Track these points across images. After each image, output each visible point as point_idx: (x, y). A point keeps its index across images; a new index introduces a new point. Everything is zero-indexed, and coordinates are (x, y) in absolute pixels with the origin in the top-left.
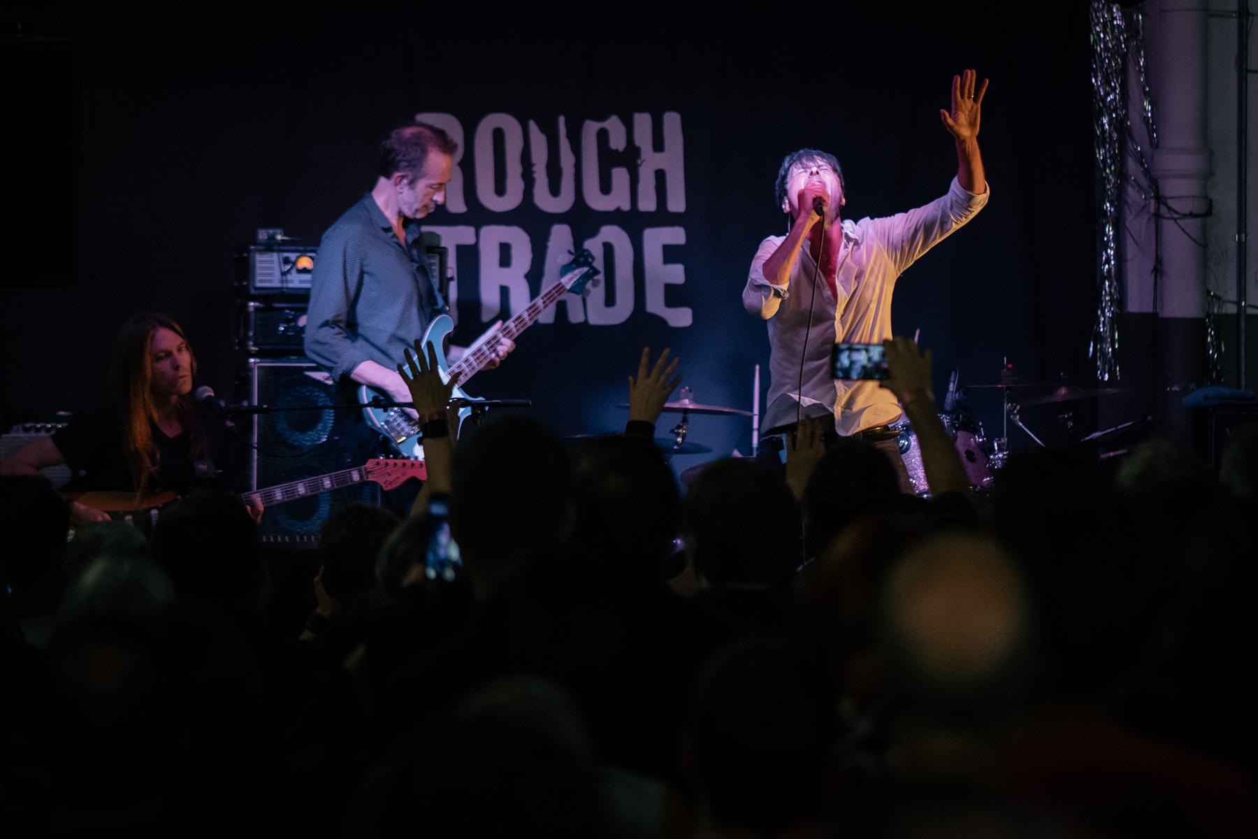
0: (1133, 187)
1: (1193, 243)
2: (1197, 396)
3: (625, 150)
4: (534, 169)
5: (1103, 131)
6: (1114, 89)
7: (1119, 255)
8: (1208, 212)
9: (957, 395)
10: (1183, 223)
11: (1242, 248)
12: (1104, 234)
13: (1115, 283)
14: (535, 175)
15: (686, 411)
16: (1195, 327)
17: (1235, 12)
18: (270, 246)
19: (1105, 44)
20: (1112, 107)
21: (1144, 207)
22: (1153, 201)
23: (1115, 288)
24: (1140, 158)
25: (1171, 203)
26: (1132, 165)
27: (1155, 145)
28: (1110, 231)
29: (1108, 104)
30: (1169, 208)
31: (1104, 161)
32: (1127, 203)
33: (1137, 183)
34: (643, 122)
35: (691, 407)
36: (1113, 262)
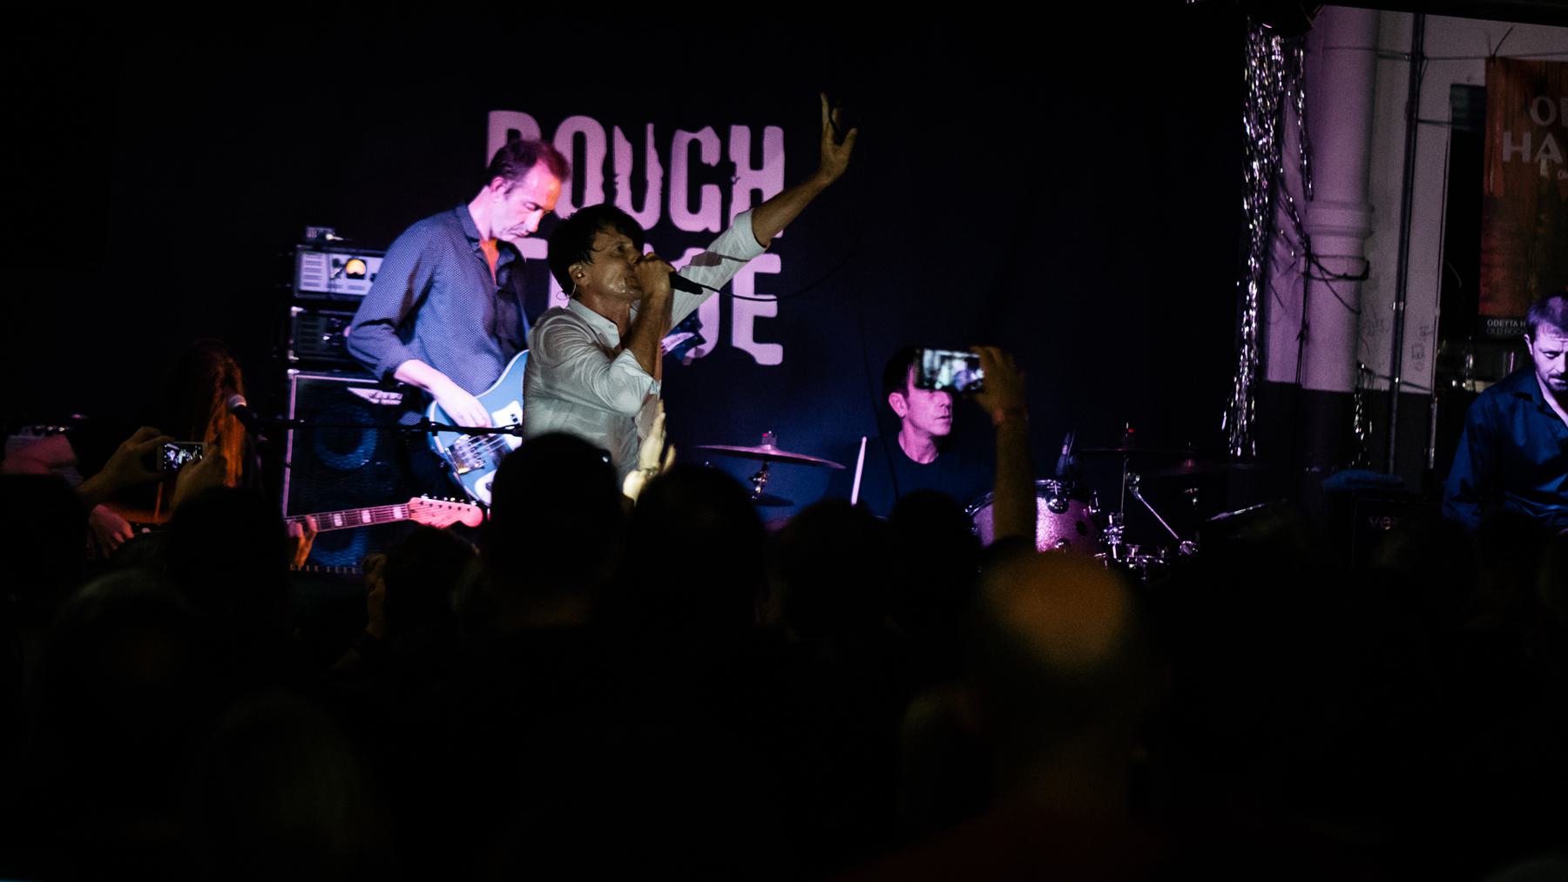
0: (1282, 243)
1: (1347, 310)
2: (1339, 479)
3: (719, 163)
4: (617, 180)
5: (1253, 178)
6: (1269, 129)
7: (1263, 319)
8: (1363, 275)
9: (1071, 459)
10: (1334, 285)
11: (1400, 318)
12: (1248, 293)
13: (1255, 347)
14: (618, 187)
15: (767, 457)
16: (1340, 402)
17: (1408, 55)
18: (320, 246)
19: (1260, 82)
20: (1264, 152)
21: (1291, 267)
22: (1303, 259)
23: (1255, 354)
24: (1292, 210)
25: (1322, 262)
26: (1282, 217)
27: (1310, 197)
28: (1253, 290)
29: (1259, 148)
30: (1321, 268)
31: (1251, 210)
32: (1273, 259)
33: (1287, 239)
34: (740, 137)
35: (773, 453)
36: (1254, 325)
